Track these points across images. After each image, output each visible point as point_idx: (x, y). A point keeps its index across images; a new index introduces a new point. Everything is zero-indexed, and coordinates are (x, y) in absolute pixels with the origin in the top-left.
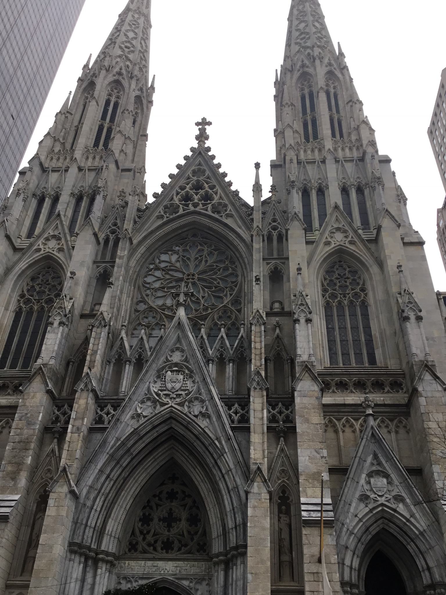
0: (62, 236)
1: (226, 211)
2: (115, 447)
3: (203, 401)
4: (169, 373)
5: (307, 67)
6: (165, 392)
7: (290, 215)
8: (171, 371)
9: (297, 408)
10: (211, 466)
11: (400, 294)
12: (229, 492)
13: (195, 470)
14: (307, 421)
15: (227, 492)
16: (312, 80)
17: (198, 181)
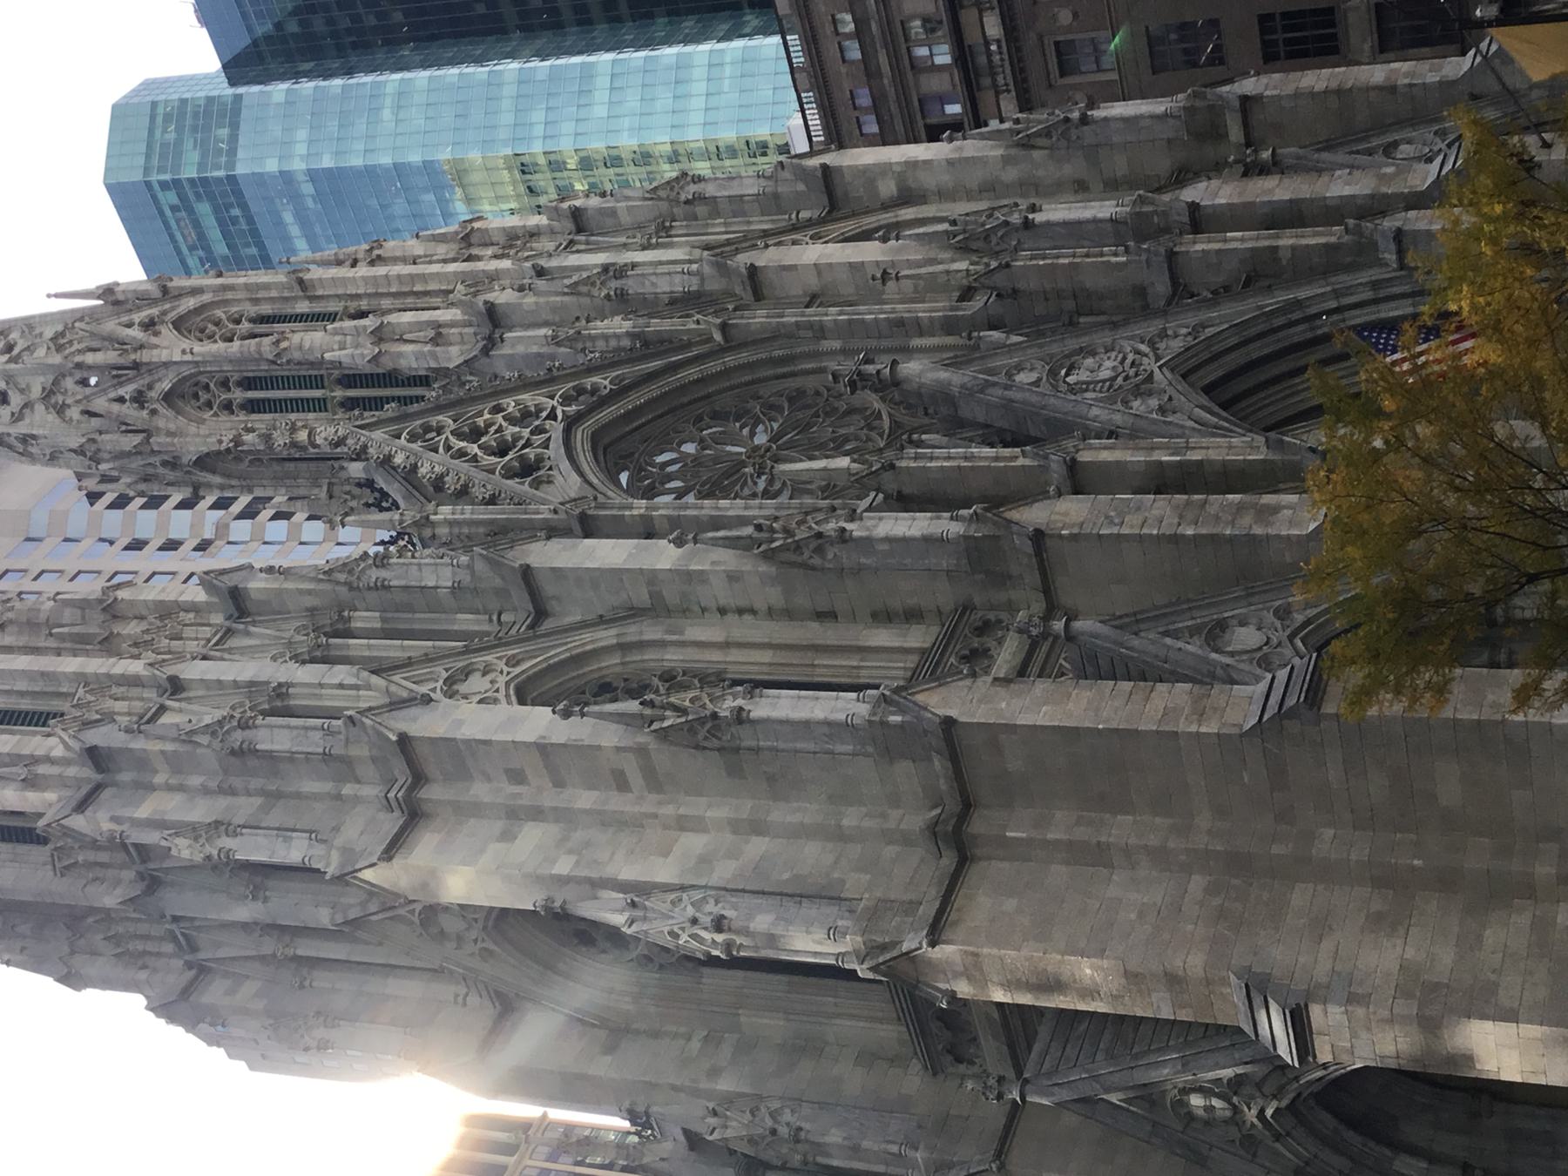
0: (461, 664)
1: (595, 390)
2: (1232, 427)
3: (1163, 334)
4: (1069, 379)
5: (164, 313)
6: (1120, 380)
7: (694, 288)
8: (1067, 375)
9: (1235, 201)
10: (1309, 335)
11: (1018, 133)
12: (1376, 301)
13: (1298, 392)
14: (1271, 191)
15: (1373, 308)
16: (219, 313)
17: (457, 434)
